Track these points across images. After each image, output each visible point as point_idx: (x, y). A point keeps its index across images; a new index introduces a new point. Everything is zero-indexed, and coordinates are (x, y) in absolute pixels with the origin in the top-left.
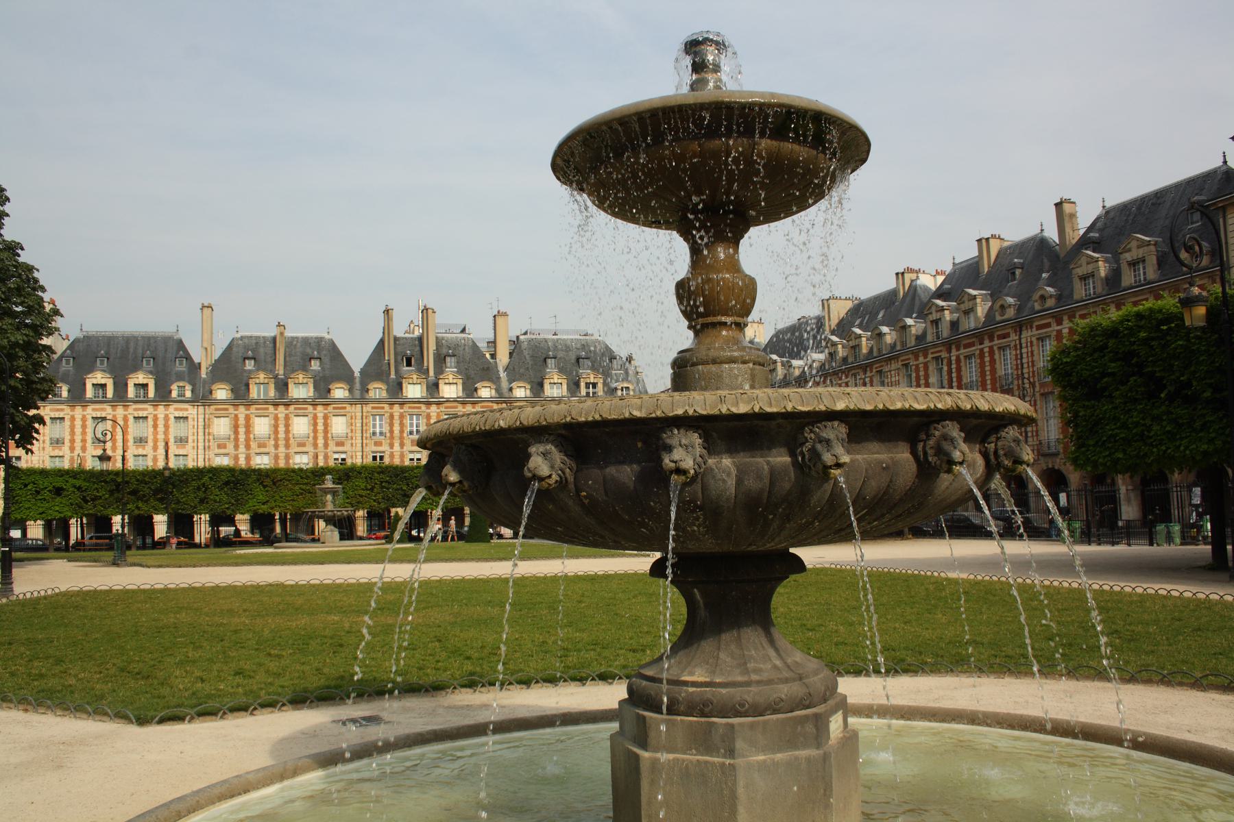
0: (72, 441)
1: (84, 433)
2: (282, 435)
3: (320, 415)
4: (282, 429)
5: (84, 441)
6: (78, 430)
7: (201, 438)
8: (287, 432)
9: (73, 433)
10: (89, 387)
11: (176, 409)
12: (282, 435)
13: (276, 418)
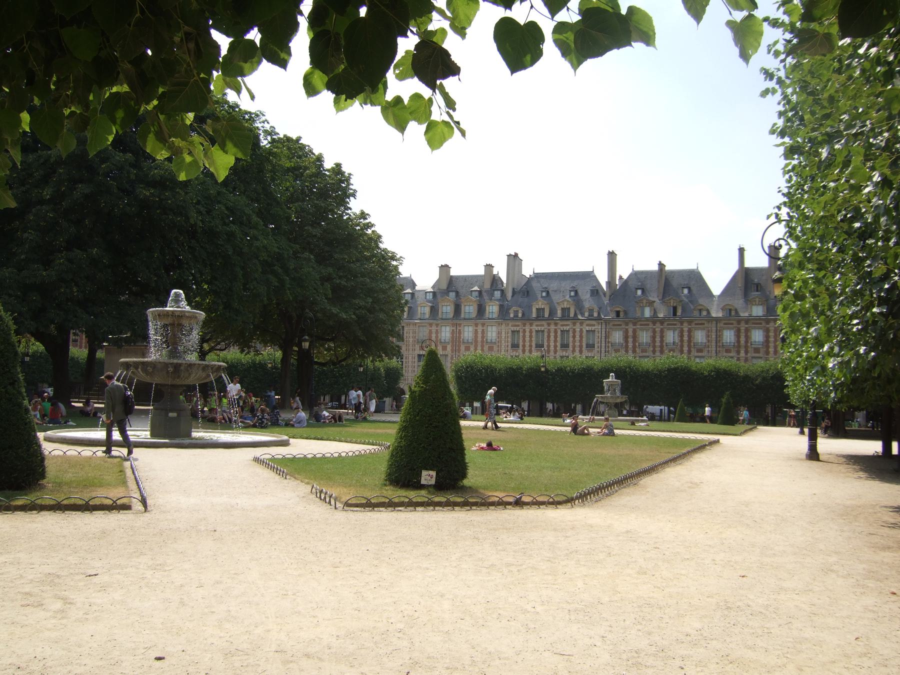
0: (524, 346)
1: (531, 341)
2: (658, 344)
3: (686, 329)
4: (658, 339)
5: (531, 346)
6: (527, 339)
7: (603, 345)
8: (662, 341)
9: (524, 341)
10: (534, 310)
11: (587, 325)
12: (658, 344)
13: (654, 332)
